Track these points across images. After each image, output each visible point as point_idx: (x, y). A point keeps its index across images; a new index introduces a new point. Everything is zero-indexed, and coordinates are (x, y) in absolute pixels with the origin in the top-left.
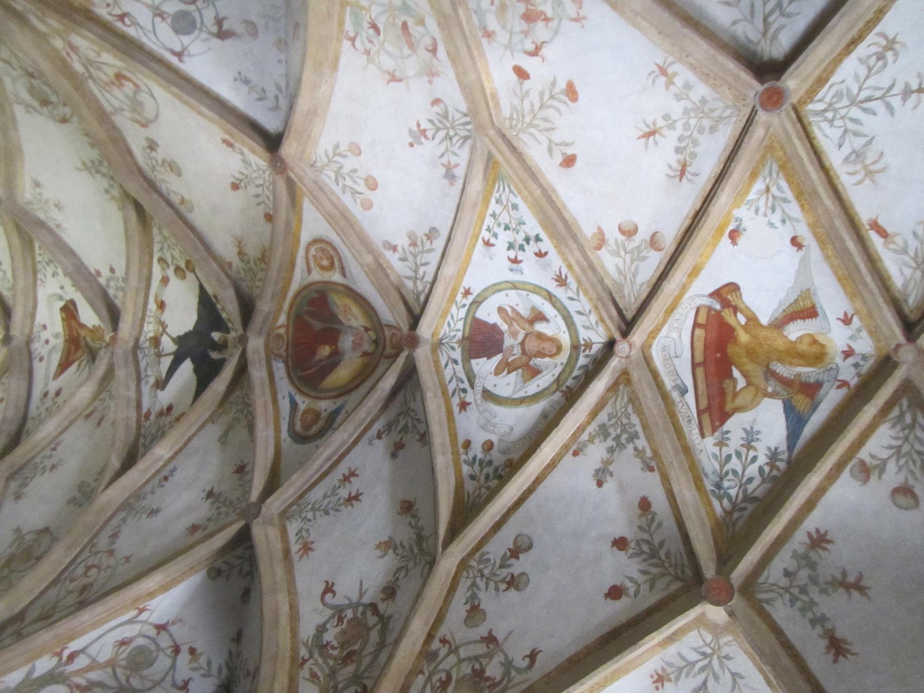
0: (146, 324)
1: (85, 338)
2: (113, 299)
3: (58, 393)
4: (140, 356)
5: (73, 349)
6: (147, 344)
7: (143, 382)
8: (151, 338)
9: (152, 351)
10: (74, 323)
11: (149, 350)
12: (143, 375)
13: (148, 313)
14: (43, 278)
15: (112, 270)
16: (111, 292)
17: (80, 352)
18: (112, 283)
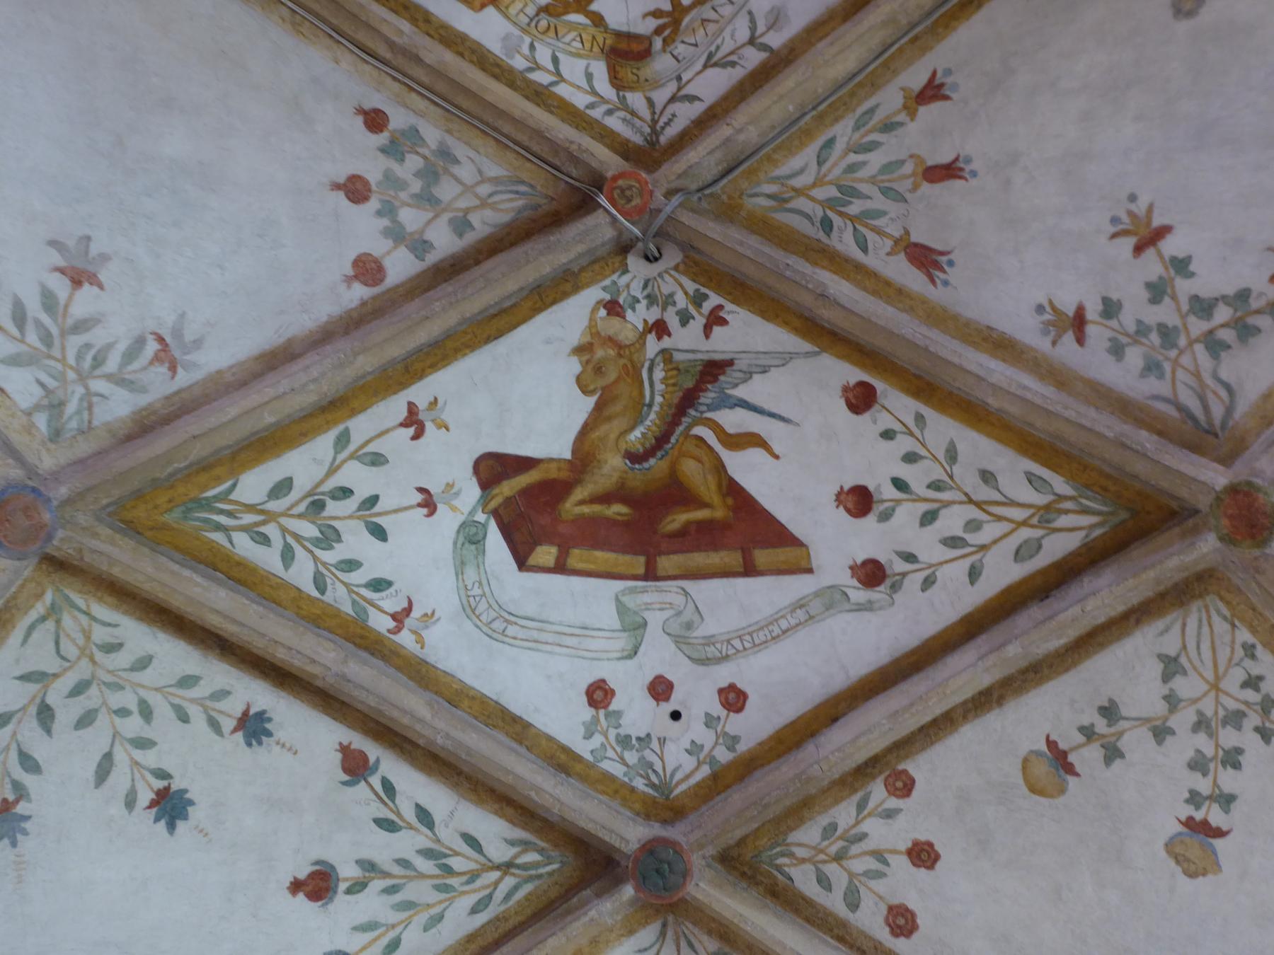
0: (562, 90)
1: (635, 458)
2: (470, 238)
3: (859, 501)
4: (685, 114)
5: (679, 519)
6: (636, 99)
7: (776, 40)
8: (617, 81)
9: (661, 64)
10: (573, 506)
11: (657, 84)
12: (754, 58)
13: (519, 63)
14: (392, 603)
15: (355, 190)
16: (444, 242)
17: (692, 470)
18: (411, 218)
